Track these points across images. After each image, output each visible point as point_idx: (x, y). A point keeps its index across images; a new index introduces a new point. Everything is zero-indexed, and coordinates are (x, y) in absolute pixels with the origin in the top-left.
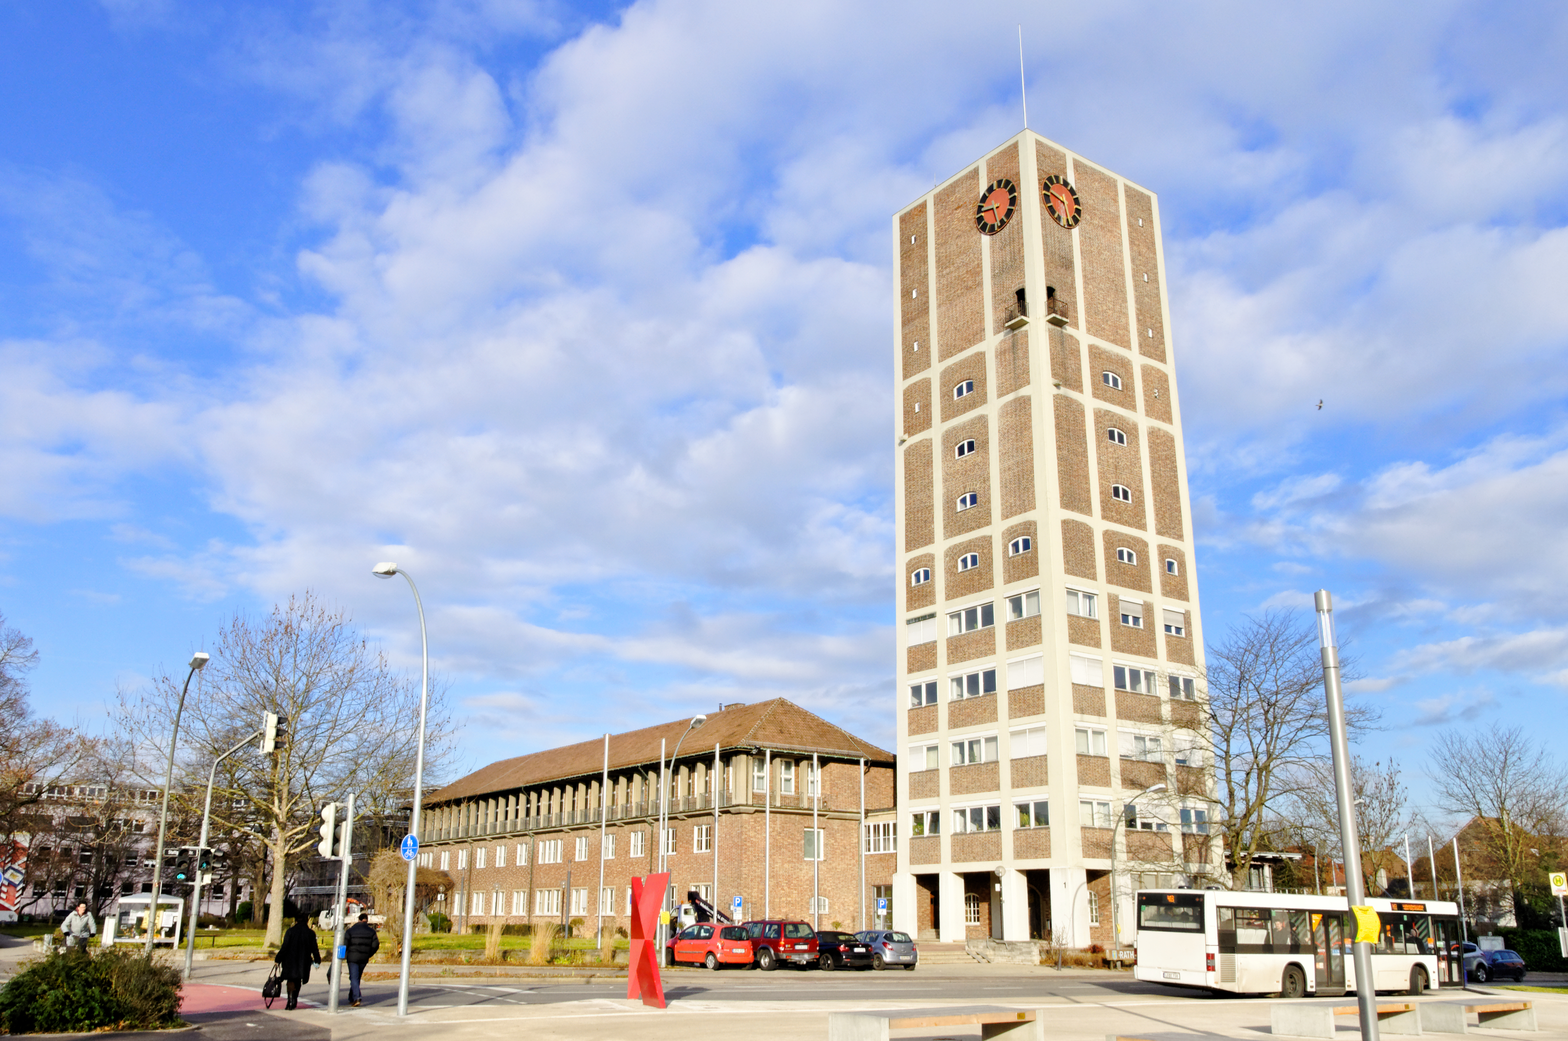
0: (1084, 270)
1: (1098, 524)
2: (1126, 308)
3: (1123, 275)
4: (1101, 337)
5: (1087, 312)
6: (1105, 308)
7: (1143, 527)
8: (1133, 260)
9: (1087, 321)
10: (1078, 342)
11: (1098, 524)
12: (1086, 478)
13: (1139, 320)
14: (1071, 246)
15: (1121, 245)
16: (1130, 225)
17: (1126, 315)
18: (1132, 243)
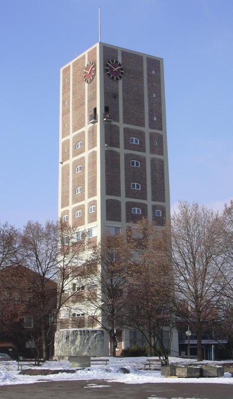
0: (124, 97)
1: (123, 199)
2: (144, 110)
3: (143, 96)
4: (130, 124)
5: (124, 114)
6: (133, 111)
7: (146, 199)
8: (149, 89)
9: (124, 118)
10: (118, 127)
11: (123, 199)
12: (119, 182)
13: (149, 114)
14: (118, 88)
15: (143, 83)
16: (149, 75)
17: (143, 113)
18: (149, 82)
